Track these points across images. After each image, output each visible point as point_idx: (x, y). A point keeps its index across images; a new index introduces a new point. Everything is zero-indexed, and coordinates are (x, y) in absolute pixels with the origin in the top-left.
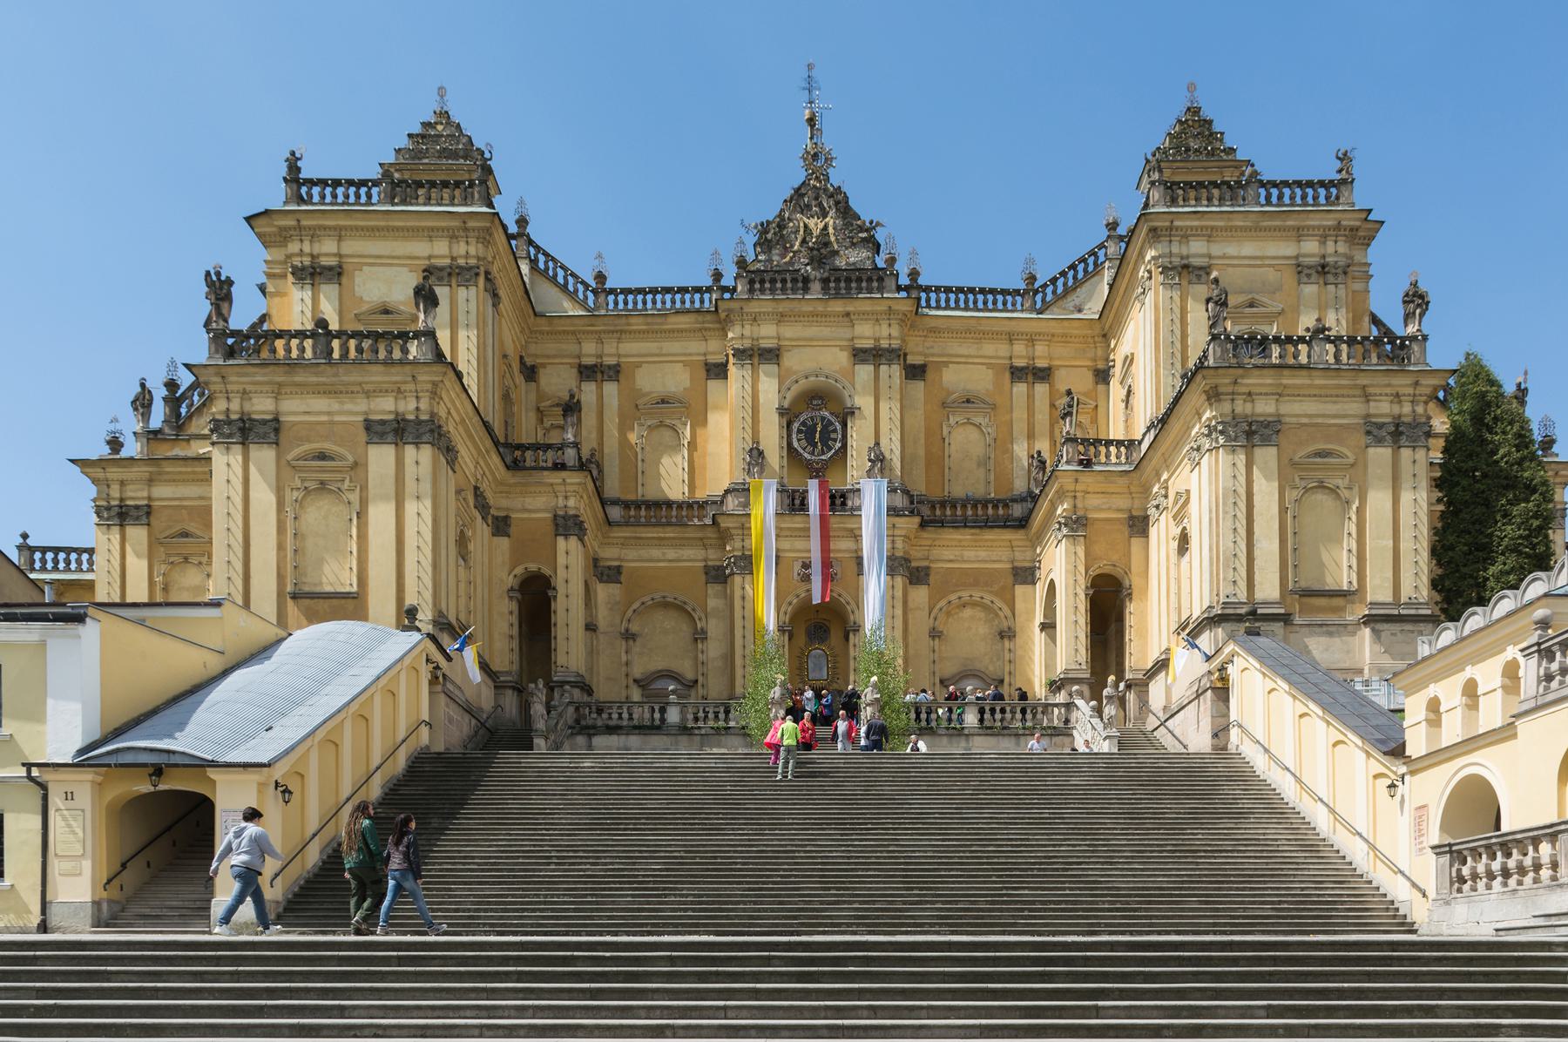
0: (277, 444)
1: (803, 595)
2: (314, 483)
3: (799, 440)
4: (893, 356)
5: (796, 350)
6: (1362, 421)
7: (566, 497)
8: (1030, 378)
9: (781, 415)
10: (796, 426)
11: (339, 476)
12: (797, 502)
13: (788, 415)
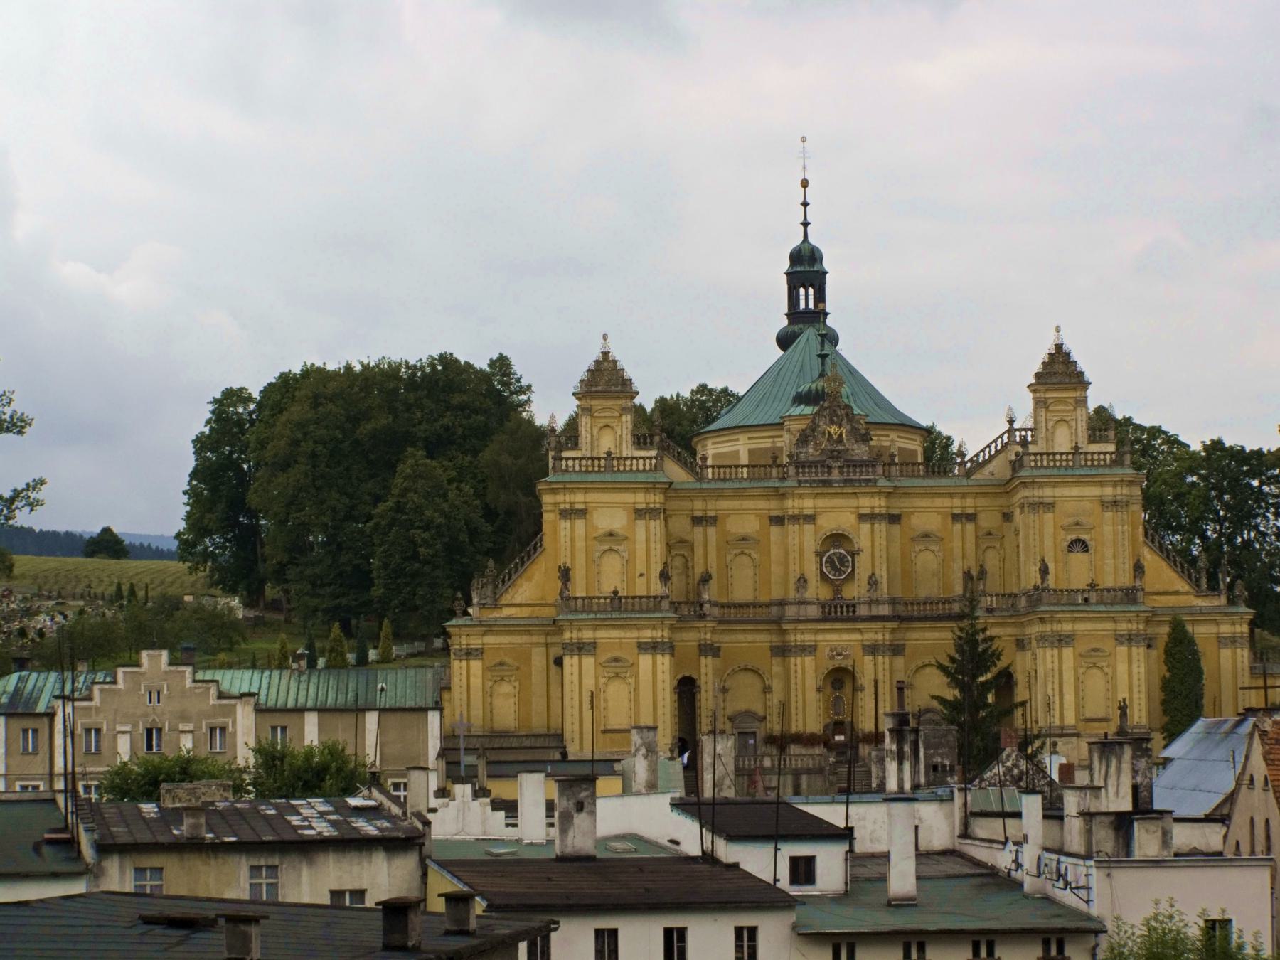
3: (826, 567)
8: (964, 520)
10: (824, 559)
11: (624, 670)
12: (827, 610)
13: (820, 555)
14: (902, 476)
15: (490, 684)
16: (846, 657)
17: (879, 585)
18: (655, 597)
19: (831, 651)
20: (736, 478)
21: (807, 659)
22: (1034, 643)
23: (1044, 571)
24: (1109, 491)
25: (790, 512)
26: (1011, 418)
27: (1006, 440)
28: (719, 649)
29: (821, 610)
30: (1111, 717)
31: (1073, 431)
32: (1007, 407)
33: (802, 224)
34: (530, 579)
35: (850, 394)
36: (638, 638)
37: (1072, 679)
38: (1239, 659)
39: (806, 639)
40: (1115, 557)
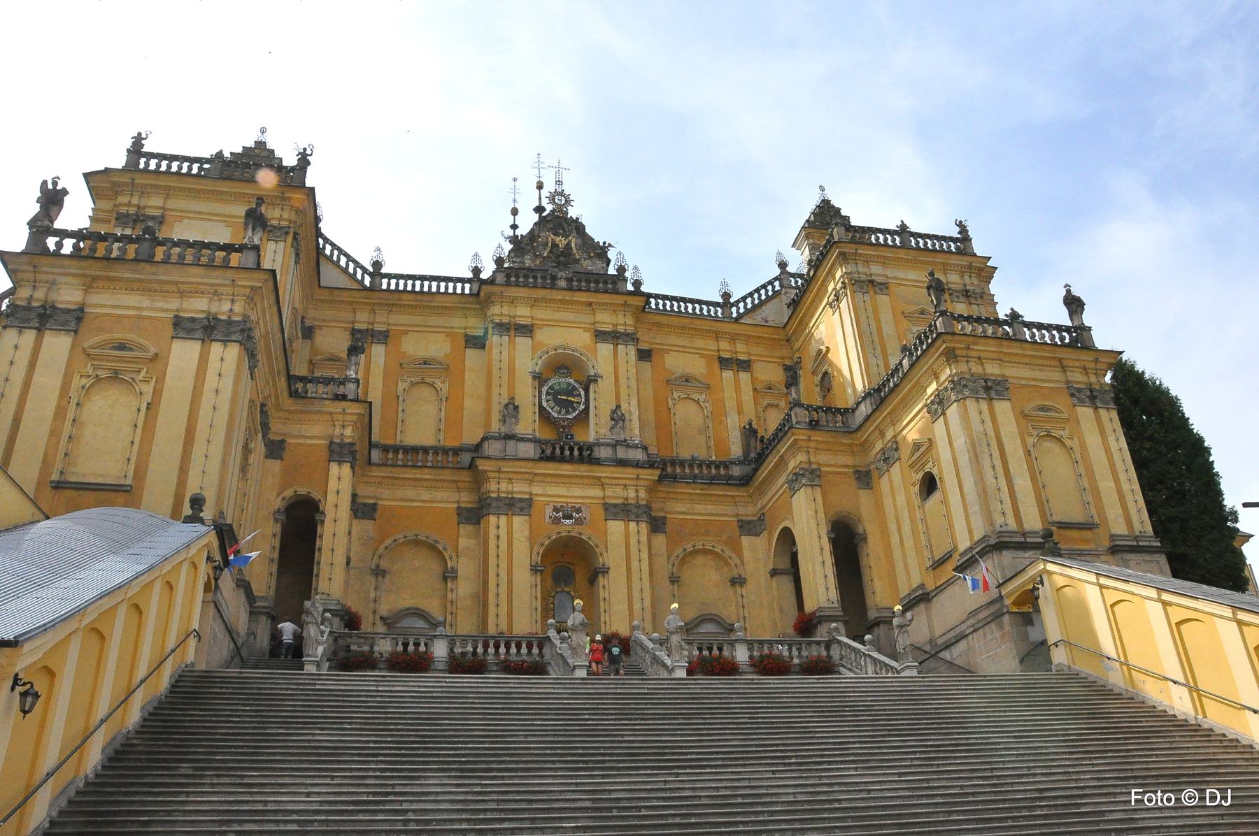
0: (76, 332)
1: (554, 537)
2: (106, 371)
3: (547, 401)
4: (628, 339)
5: (546, 329)
6: (1064, 386)
7: (343, 426)
8: (735, 367)
9: (534, 378)
10: (545, 389)
12: (549, 452)
13: (539, 379)
16: (579, 522)
17: (627, 423)
19: (556, 510)
27: (777, 288)
28: (374, 507)
30: (1096, 520)
32: (776, 252)
36: (177, 310)
37: (1021, 452)
39: (515, 489)
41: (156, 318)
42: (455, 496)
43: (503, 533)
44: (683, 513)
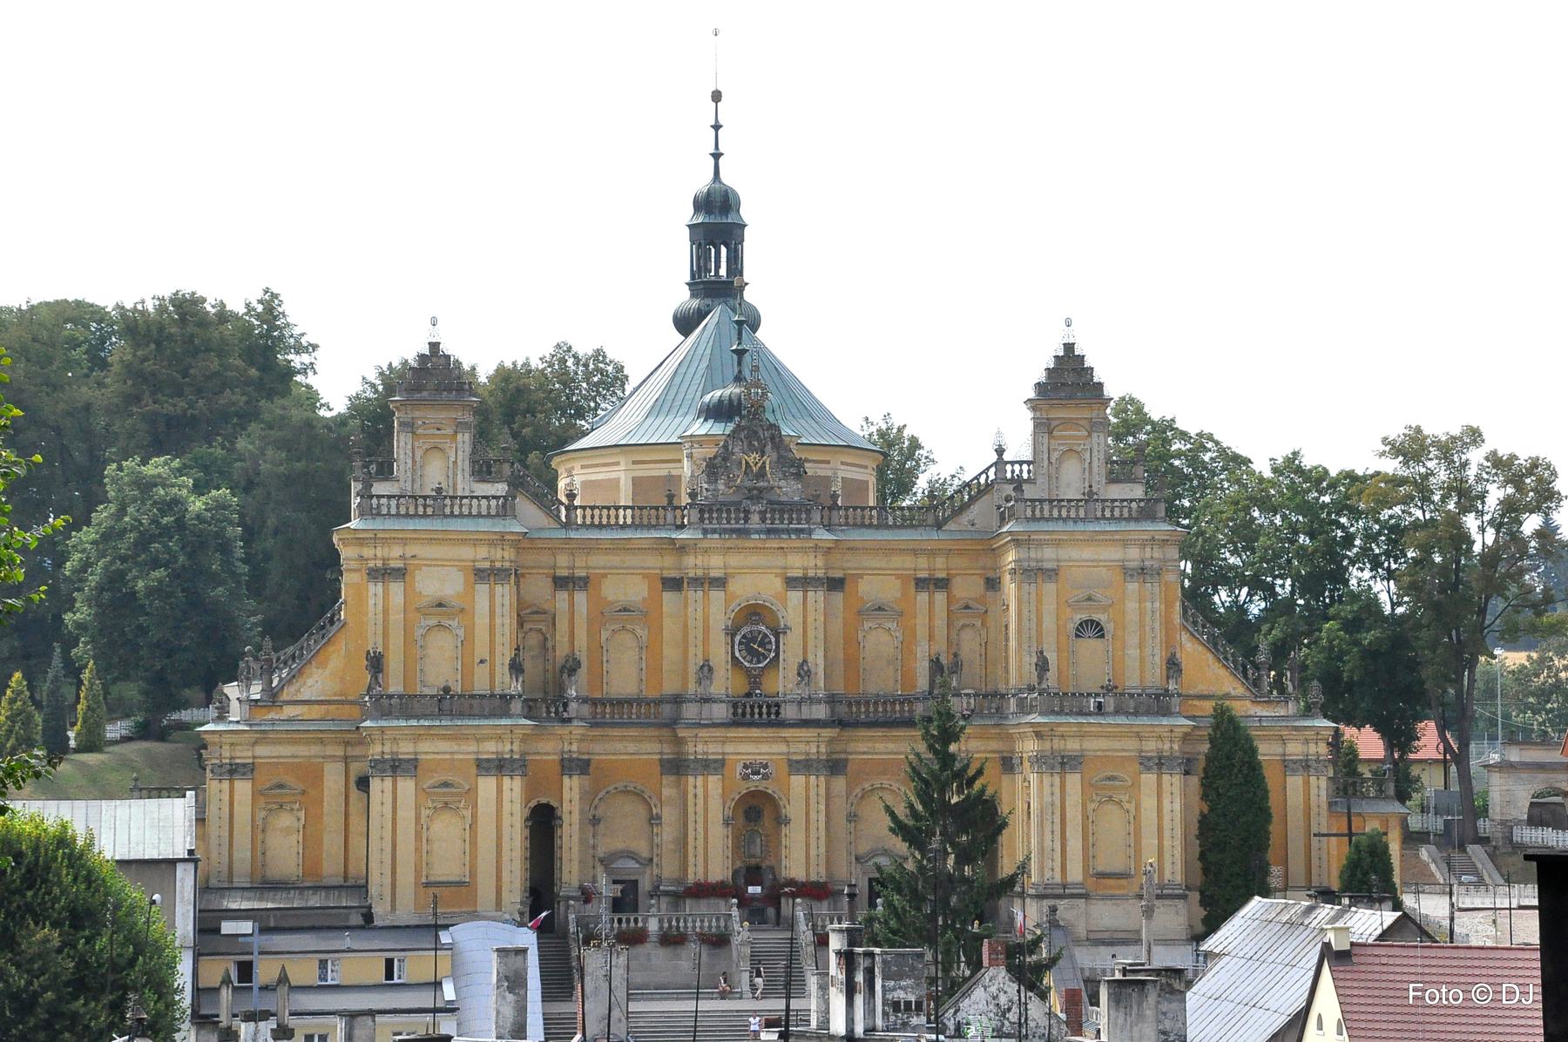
8: (931, 587)
10: (738, 638)
12: (740, 711)
13: (731, 632)
14: (847, 524)
15: (263, 814)
16: (766, 777)
17: (812, 676)
18: (503, 697)
19: (746, 766)
20: (617, 523)
21: (711, 778)
22: (1027, 764)
23: (1042, 666)
24: (1133, 553)
25: (691, 575)
26: (1000, 445)
27: (992, 476)
29: (731, 711)
30: (1133, 872)
31: (1087, 465)
32: (995, 430)
33: (712, 155)
34: (323, 665)
35: (776, 406)
36: (478, 753)
38: (1314, 791)
40: (1141, 646)
41: (462, 760)
42: (656, 747)
43: (700, 792)
44: (864, 753)
